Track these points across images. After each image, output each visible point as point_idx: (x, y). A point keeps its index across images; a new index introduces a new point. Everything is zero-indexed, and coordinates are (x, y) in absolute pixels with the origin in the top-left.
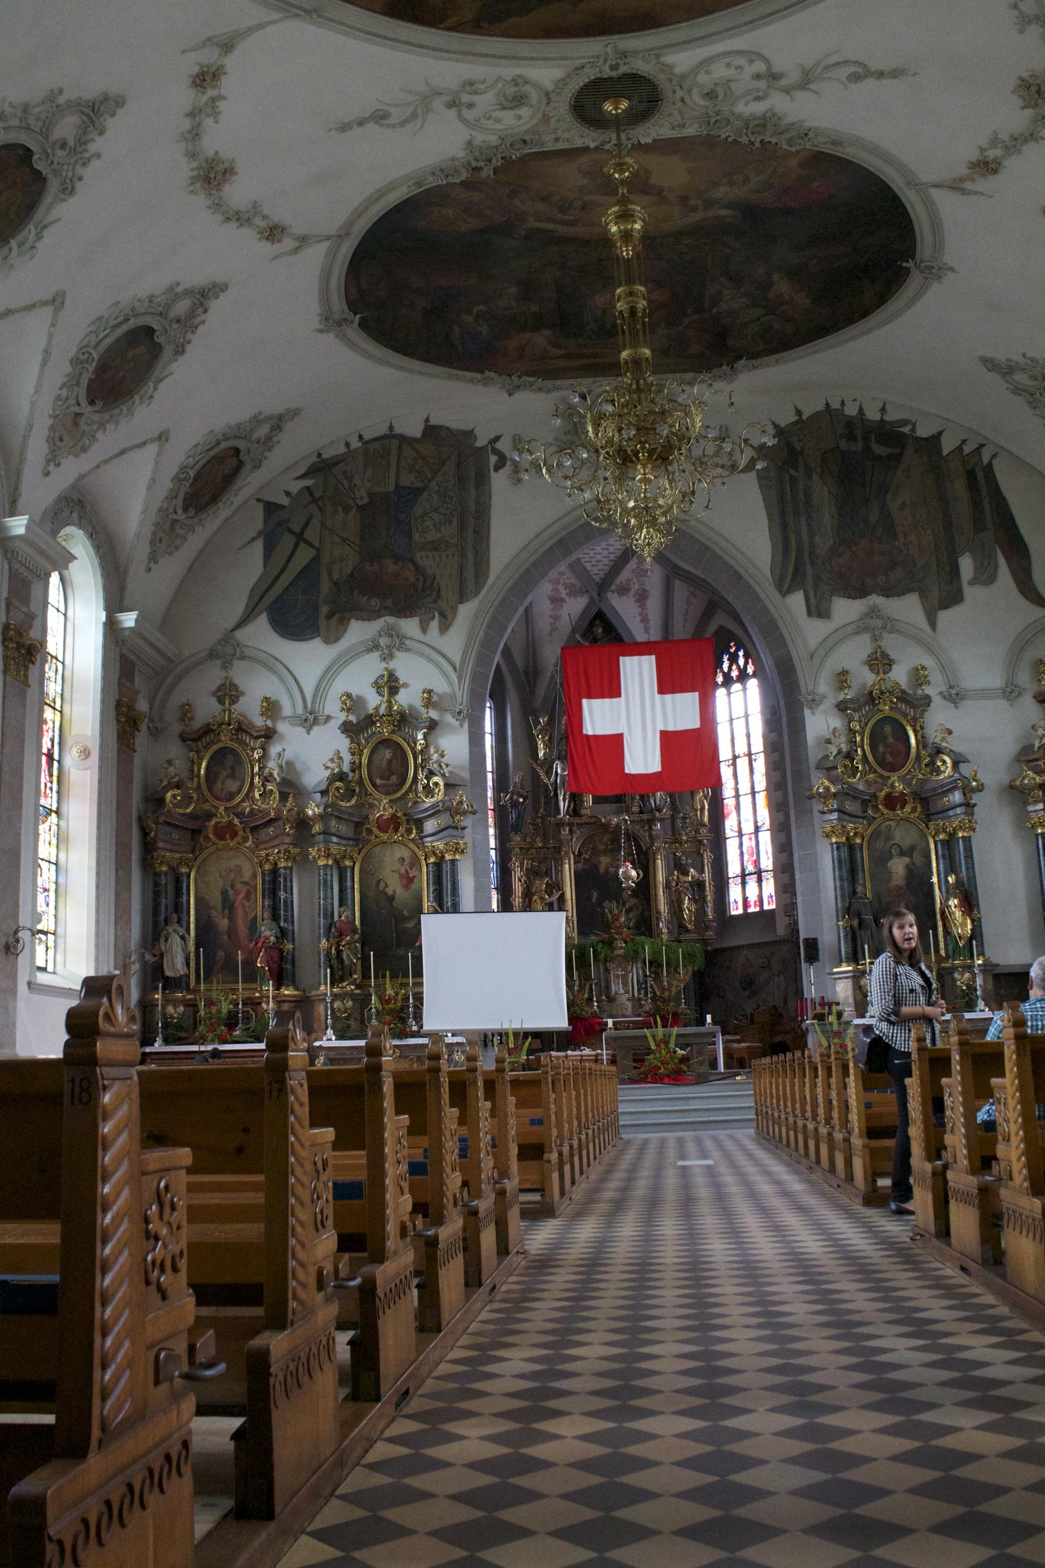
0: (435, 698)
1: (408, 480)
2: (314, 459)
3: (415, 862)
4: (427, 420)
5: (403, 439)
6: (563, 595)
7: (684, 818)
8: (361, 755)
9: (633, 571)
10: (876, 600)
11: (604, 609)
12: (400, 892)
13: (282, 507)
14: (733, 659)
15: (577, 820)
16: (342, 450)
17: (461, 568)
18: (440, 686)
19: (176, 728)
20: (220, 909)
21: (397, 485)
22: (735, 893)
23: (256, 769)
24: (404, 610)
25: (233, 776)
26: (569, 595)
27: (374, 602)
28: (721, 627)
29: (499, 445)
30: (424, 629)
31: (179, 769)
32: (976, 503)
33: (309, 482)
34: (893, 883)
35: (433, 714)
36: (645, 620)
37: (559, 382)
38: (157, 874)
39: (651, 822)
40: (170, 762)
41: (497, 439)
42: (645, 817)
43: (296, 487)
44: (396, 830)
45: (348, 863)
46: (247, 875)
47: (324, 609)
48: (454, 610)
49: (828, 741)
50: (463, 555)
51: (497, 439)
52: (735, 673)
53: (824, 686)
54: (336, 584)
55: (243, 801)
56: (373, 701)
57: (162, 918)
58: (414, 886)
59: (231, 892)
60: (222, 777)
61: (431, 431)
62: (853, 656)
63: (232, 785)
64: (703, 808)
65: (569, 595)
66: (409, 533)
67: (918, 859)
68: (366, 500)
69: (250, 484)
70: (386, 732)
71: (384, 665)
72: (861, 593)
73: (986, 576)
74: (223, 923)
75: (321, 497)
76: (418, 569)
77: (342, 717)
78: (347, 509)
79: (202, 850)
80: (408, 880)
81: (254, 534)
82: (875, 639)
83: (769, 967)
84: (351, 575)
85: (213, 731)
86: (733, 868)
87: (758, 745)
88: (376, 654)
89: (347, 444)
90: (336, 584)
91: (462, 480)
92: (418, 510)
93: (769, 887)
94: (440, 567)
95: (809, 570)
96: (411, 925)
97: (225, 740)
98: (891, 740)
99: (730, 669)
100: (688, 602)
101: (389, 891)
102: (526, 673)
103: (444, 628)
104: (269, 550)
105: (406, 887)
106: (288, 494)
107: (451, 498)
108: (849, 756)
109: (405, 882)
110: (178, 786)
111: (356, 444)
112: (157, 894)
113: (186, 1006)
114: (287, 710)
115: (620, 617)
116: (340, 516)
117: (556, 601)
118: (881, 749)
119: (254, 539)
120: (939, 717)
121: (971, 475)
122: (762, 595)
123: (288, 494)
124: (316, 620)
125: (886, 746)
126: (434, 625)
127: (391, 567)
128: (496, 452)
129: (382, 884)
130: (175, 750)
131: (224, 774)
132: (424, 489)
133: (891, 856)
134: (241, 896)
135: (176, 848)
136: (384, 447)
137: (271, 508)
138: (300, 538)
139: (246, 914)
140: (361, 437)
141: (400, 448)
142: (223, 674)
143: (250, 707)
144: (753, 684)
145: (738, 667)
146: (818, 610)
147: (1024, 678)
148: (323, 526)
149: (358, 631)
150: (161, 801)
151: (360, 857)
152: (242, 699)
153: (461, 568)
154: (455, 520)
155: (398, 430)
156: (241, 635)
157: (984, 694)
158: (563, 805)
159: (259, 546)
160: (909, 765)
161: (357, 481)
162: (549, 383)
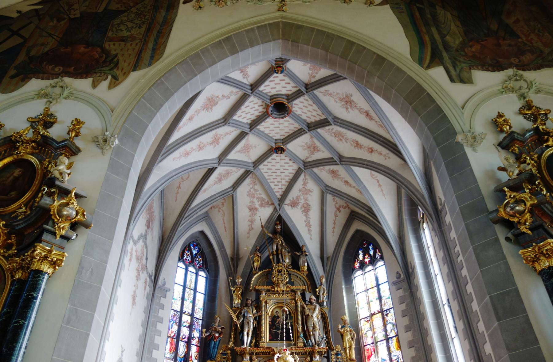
0: (83, 131)
6: (257, 206)
7: (337, 354)
9: (300, 190)
11: (283, 215)
15: (256, 350)
26: (261, 205)
28: (357, 231)
35: (78, 142)
36: (308, 225)
42: (308, 350)
48: (126, 74)
52: (367, 260)
64: (350, 347)
65: (261, 205)
68: (78, 15)
72: (497, 67)
87: (388, 304)
99: (364, 258)
100: (336, 216)
102: (232, 259)
115: (292, 222)
117: (253, 210)
122: (404, 69)
127: (82, 49)
145: (370, 255)
149: (35, 85)
158: (247, 339)
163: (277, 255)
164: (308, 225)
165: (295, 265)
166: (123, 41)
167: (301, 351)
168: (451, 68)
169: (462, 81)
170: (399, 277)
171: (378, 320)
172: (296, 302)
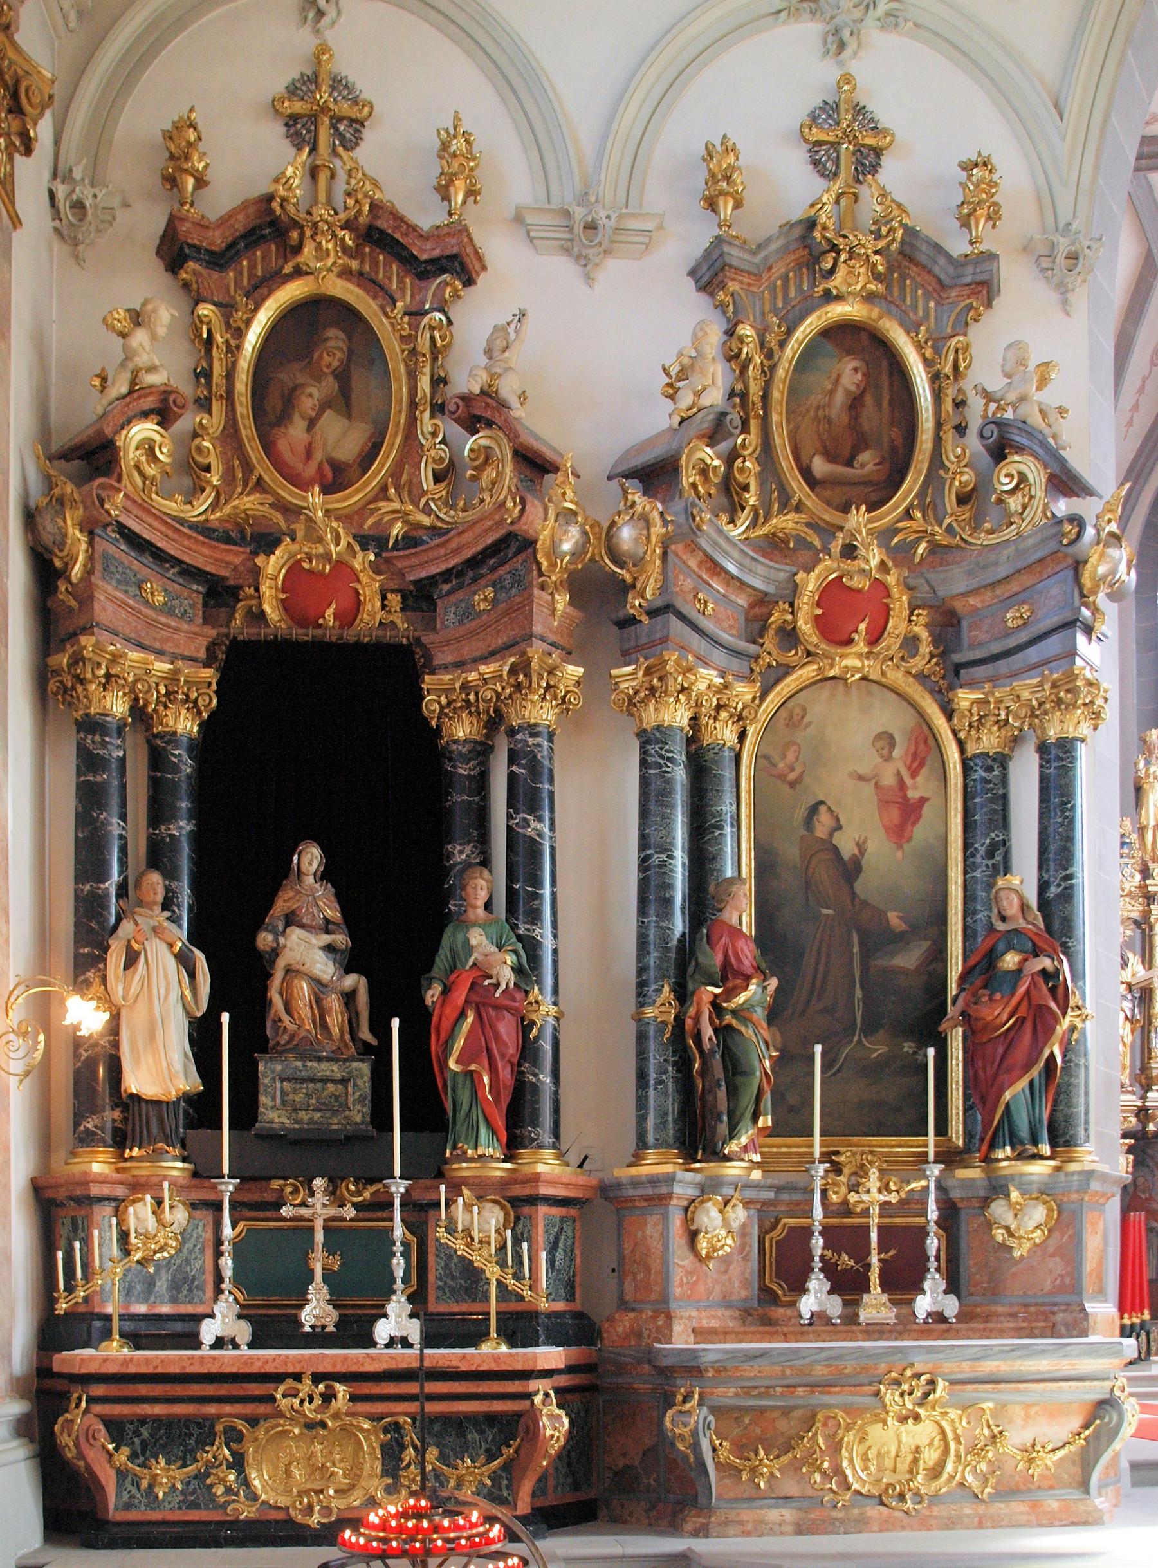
23: (424, 383)
25: (343, 401)
38: (91, 725)
55: (382, 493)
57: (111, 884)
58: (921, 832)
63: (341, 438)
80: (905, 812)
105: (899, 832)
109: (895, 814)
112: (90, 799)
129: (824, 819)
131: (311, 396)
152: (371, 136)
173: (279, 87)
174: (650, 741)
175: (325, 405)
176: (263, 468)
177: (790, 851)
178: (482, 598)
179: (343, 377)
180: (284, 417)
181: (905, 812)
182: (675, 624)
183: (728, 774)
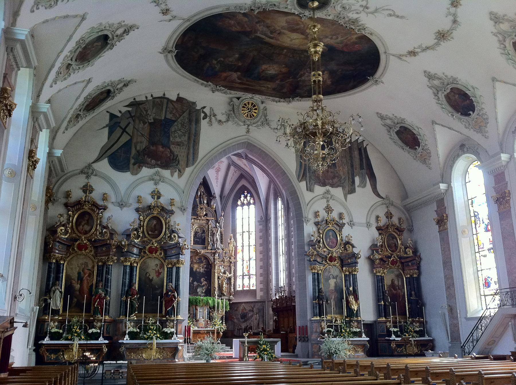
1: (169, 116)
2: (133, 100)
3: (162, 266)
4: (178, 95)
5: (168, 99)
8: (144, 222)
10: (328, 187)
12: (155, 278)
13: (118, 117)
14: (246, 197)
16: (144, 99)
17: (188, 154)
18: (177, 198)
19: (64, 201)
20: (76, 280)
21: (165, 117)
22: (239, 282)
23: (99, 222)
24: (165, 166)
25: (87, 224)
27: (153, 162)
29: (204, 110)
30: (172, 175)
31: (63, 219)
32: (361, 160)
33: (130, 109)
34: (330, 288)
35: (174, 208)
36: (217, 179)
37: (232, 92)
39: (214, 254)
40: (61, 215)
41: (204, 107)
42: (213, 251)
43: (124, 110)
44: (156, 253)
45: (135, 265)
46: (90, 267)
47: (132, 161)
48: (184, 169)
49: (312, 236)
50: (189, 149)
51: (204, 107)
52: (245, 202)
53: (311, 216)
54: (138, 151)
56: (150, 200)
58: (161, 276)
59: (82, 273)
60: (83, 224)
61: (180, 100)
62: (320, 206)
63: (87, 228)
64: (232, 250)
66: (169, 137)
67: (338, 280)
68: (152, 121)
69: (108, 105)
70: (155, 213)
71: (155, 187)
72: (324, 185)
73: (363, 185)
74: (78, 286)
75: (134, 116)
76: (172, 152)
77: (137, 205)
78: (144, 123)
79: (70, 254)
80: (159, 273)
81: (105, 125)
82: (328, 201)
83: (253, 311)
84: (144, 149)
85: (81, 204)
86: (239, 273)
87: (253, 229)
88: (152, 182)
89: (146, 97)
90: (138, 151)
91: (190, 121)
92: (173, 129)
93: (253, 280)
94: (180, 152)
95: (308, 174)
96: (158, 292)
97: (86, 208)
98: (332, 237)
100: (233, 175)
101: (151, 277)
103: (180, 176)
104: (110, 133)
105: (158, 276)
106: (120, 112)
107: (186, 126)
108: (319, 242)
110: (63, 226)
111: (150, 98)
113: (58, 322)
114: (113, 199)
116: (141, 125)
118: (328, 240)
119: (104, 127)
120: (346, 231)
121: (360, 150)
123: (120, 112)
124: (129, 164)
125: (330, 239)
126: (176, 174)
127: (161, 149)
128: (204, 112)
130: (61, 210)
132: (174, 121)
133: (330, 279)
134: (87, 275)
135: (60, 253)
136: (160, 102)
137: (112, 116)
138: (124, 130)
139: (88, 283)
140: (152, 96)
141: (167, 103)
142: (86, 181)
143: (96, 196)
144: (252, 207)
146: (310, 189)
147: (373, 221)
148: (134, 127)
149: (146, 172)
150: (55, 232)
151: (140, 262)
153: (188, 154)
154: (187, 135)
155: (167, 96)
156: (95, 166)
157: (361, 225)
159: (107, 129)
160: (338, 246)
161: (149, 112)
162: (228, 91)
163: (200, 198)
164: (217, 179)
165: (208, 204)
166: (178, 145)
167: (210, 251)
168: (308, 182)
169: (310, 191)
170: (262, 219)
171: (246, 235)
172: (208, 226)
173: (82, 187)
174: (125, 267)
175: (85, 224)
176: (76, 232)
177: (143, 278)
178: (104, 249)
179: (88, 221)
180: (79, 225)
181: (159, 273)
182: (129, 253)
183: (135, 269)
